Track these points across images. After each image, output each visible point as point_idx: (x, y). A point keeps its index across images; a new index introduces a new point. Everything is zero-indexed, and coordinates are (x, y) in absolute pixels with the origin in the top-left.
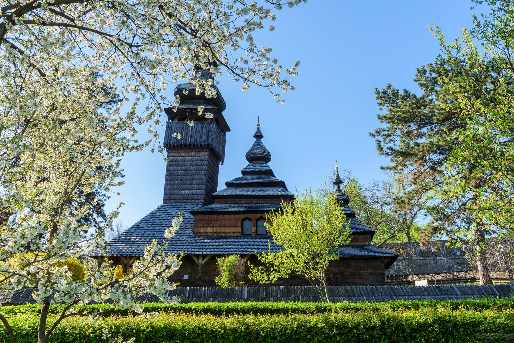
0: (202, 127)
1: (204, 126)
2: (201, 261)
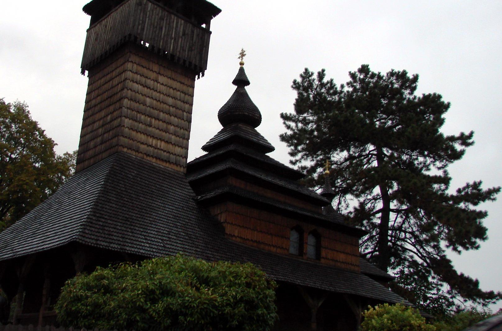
0: (193, 32)
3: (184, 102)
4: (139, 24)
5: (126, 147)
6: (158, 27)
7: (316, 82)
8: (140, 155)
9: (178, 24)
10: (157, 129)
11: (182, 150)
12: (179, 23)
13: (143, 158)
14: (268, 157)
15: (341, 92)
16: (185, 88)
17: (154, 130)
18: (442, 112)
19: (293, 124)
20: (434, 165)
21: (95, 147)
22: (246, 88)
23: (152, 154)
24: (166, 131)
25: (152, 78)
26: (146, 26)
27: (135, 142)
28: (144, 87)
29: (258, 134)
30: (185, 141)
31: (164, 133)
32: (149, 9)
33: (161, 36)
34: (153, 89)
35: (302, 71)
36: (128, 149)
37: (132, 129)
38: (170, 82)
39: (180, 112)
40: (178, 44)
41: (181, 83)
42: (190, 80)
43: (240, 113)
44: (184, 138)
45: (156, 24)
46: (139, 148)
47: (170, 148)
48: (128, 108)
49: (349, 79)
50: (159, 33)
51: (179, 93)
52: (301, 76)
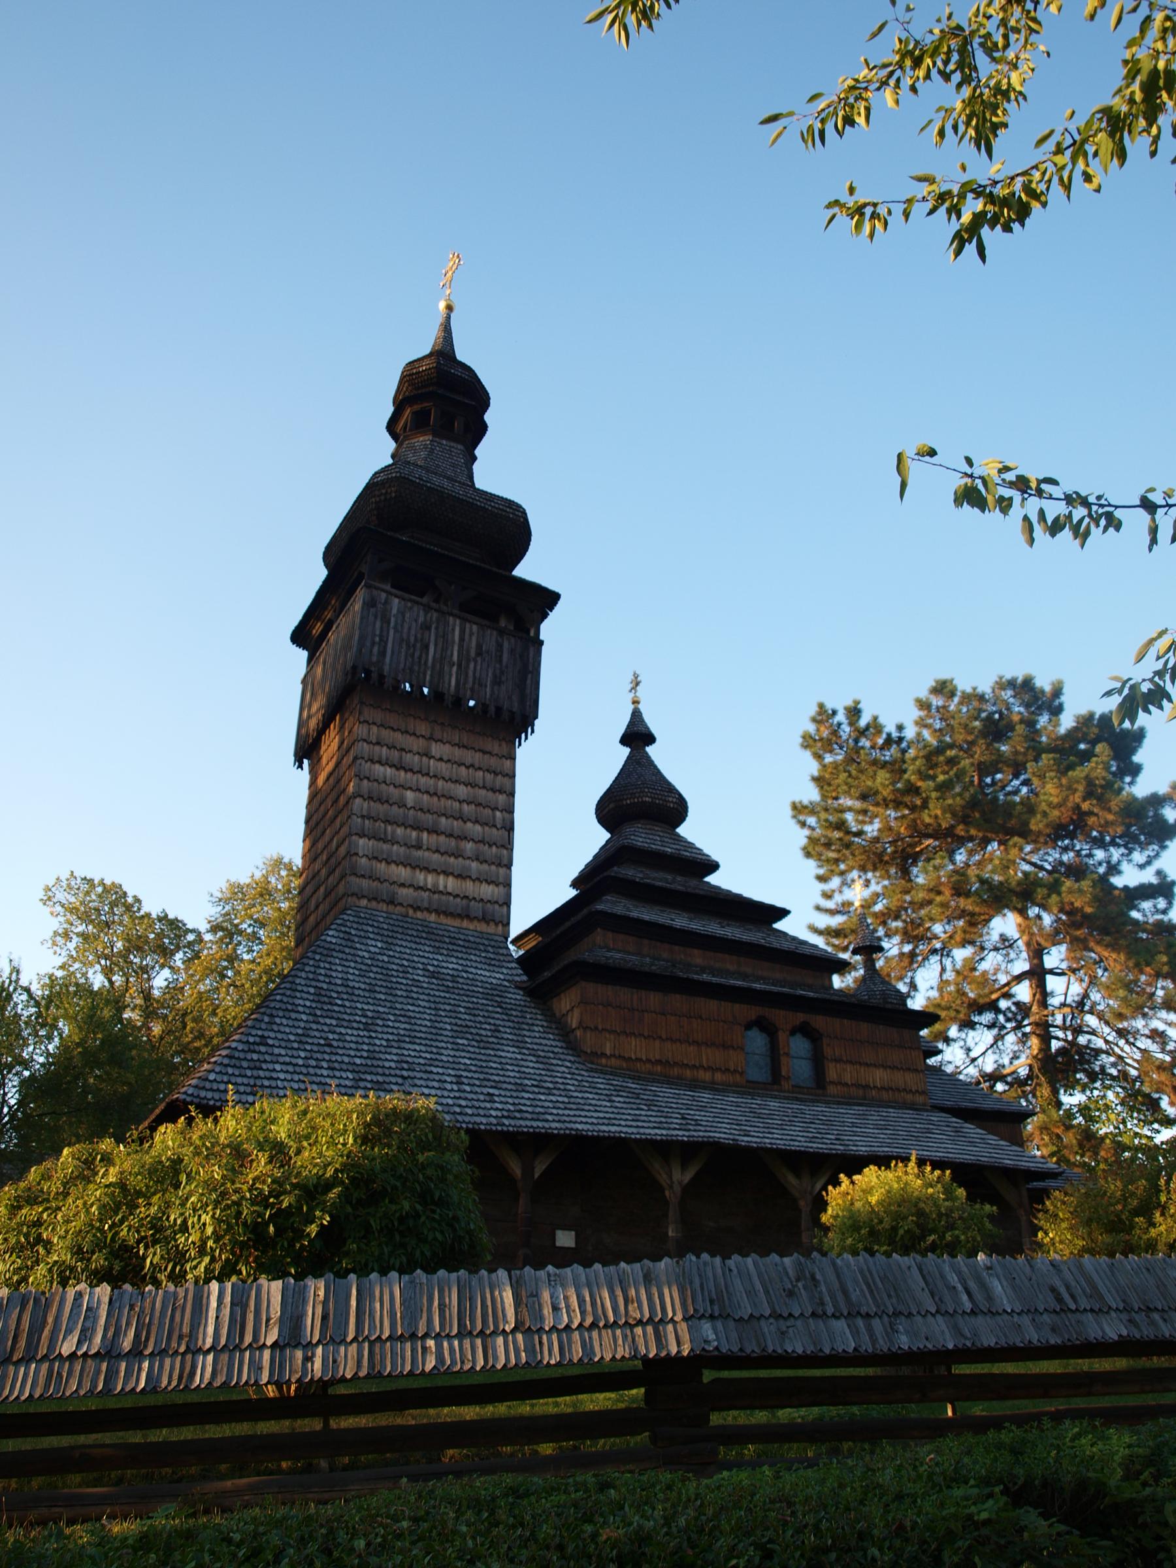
0: (500, 646)
3: (494, 790)
4: (373, 643)
5: (363, 897)
6: (418, 645)
7: (846, 728)
8: (399, 909)
9: (463, 635)
10: (434, 852)
11: (496, 889)
12: (467, 630)
13: (407, 916)
14: (708, 883)
15: (901, 739)
16: (493, 762)
17: (427, 854)
18: (1133, 751)
19: (812, 821)
20: (1130, 861)
21: (317, 907)
22: (649, 749)
23: (426, 905)
24: (457, 855)
25: (415, 749)
26: (390, 645)
27: (386, 884)
28: (398, 769)
29: (679, 839)
30: (502, 871)
31: (452, 859)
32: (394, 611)
33: (426, 663)
34: (419, 772)
35: (813, 710)
36: (369, 900)
37: (376, 858)
38: (458, 753)
39: (488, 811)
40: (467, 675)
41: (484, 752)
42: (504, 744)
43: (641, 804)
44: (499, 865)
45: (412, 639)
46: (394, 894)
47: (469, 887)
48: (363, 817)
49: (916, 713)
50: (420, 658)
51: (481, 773)
52: (814, 720)
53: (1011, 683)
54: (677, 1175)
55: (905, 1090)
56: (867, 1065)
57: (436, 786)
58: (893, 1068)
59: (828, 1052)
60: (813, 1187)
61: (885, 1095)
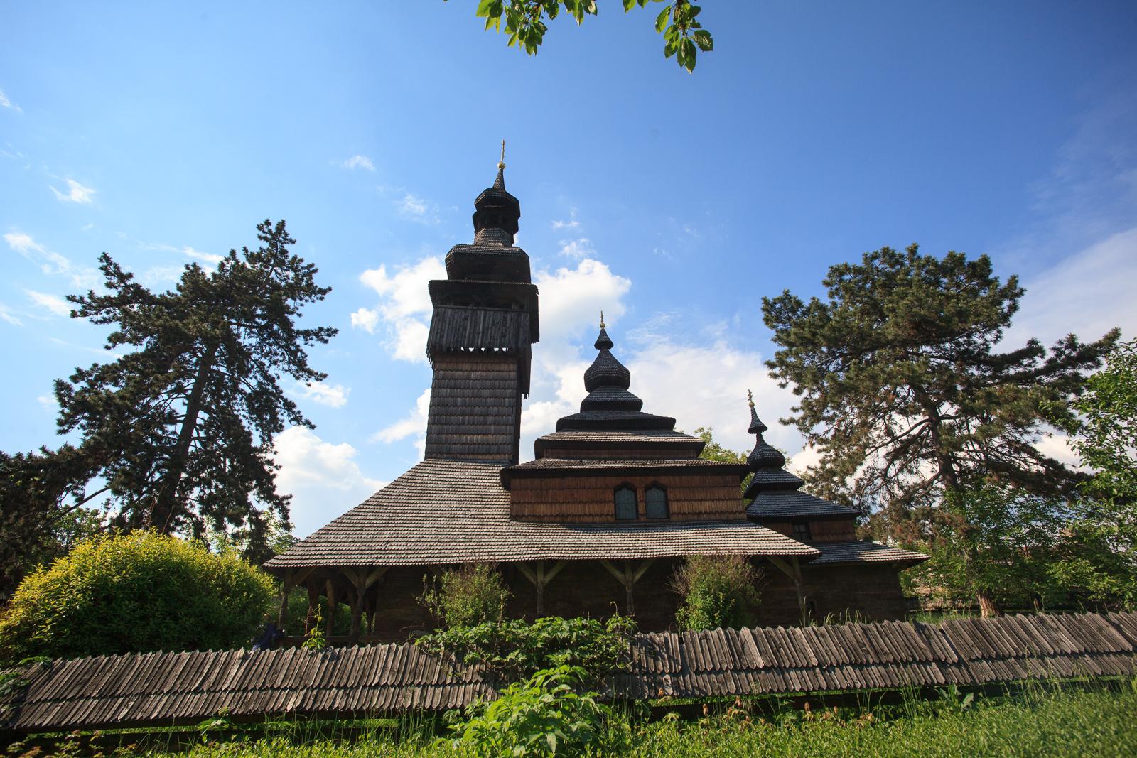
0: (505, 319)
1: (509, 317)
2: (540, 578)
24: (485, 424)
33: (465, 336)
37: (440, 433)
41: (500, 371)
43: (607, 377)
53: (875, 257)
54: (540, 578)
55: (727, 512)
56: (699, 500)
57: (473, 393)
58: (719, 500)
59: (671, 496)
60: (633, 578)
61: (713, 517)
